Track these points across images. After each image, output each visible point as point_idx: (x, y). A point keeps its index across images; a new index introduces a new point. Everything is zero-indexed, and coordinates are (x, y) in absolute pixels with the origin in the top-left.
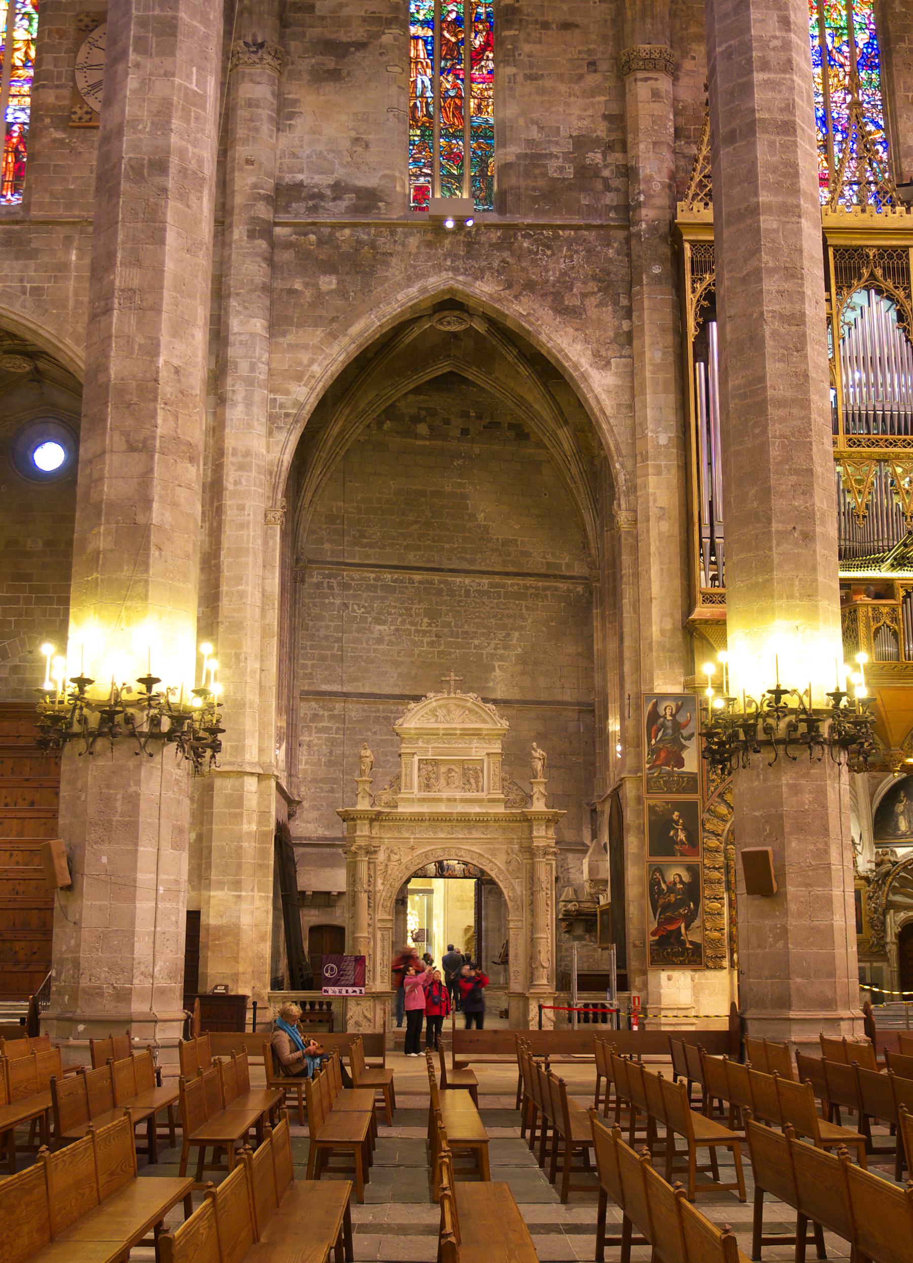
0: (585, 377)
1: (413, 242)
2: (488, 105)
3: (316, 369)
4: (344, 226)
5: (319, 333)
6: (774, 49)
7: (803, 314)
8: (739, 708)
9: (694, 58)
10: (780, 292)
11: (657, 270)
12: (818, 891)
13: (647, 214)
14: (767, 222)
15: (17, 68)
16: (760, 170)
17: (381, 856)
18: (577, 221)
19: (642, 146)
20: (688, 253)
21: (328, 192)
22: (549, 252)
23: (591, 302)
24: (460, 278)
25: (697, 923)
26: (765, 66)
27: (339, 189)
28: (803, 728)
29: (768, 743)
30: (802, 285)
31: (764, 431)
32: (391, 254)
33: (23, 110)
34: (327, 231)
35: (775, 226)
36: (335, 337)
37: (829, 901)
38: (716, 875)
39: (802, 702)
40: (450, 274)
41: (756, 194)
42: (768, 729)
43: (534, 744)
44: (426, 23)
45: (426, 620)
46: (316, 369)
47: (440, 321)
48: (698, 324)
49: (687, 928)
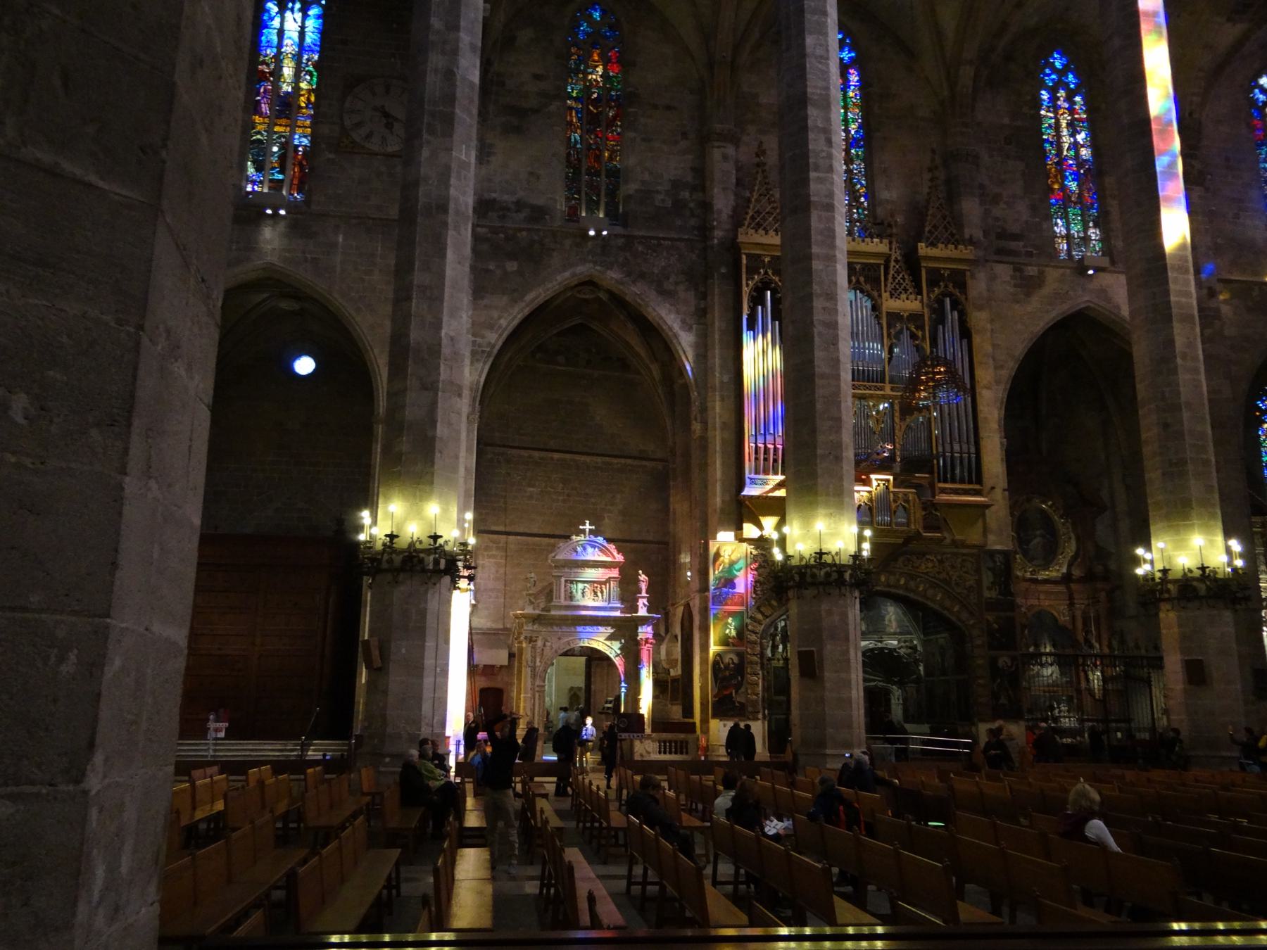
0: (676, 336)
1: (568, 243)
2: (616, 157)
3: (503, 322)
4: (521, 230)
5: (505, 299)
6: (823, 157)
7: (837, 323)
8: (794, 562)
9: (748, 134)
10: (824, 309)
11: (723, 270)
12: (843, 675)
13: (718, 234)
14: (817, 265)
15: (302, 108)
16: (813, 232)
17: (540, 643)
18: (673, 235)
19: (716, 190)
20: (744, 261)
22: (655, 254)
23: (681, 288)
24: (598, 268)
25: (743, 690)
26: (817, 169)
27: (519, 205)
28: (835, 576)
29: (813, 584)
30: (836, 305)
31: (813, 392)
32: (553, 250)
33: (305, 137)
34: (511, 232)
35: (821, 267)
36: (516, 302)
37: (850, 681)
38: (755, 658)
39: (834, 560)
40: (591, 265)
41: (810, 247)
42: (814, 576)
43: (640, 572)
44: (576, 99)
45: (561, 485)
46: (503, 322)
47: (579, 292)
48: (750, 306)
49: (736, 692)
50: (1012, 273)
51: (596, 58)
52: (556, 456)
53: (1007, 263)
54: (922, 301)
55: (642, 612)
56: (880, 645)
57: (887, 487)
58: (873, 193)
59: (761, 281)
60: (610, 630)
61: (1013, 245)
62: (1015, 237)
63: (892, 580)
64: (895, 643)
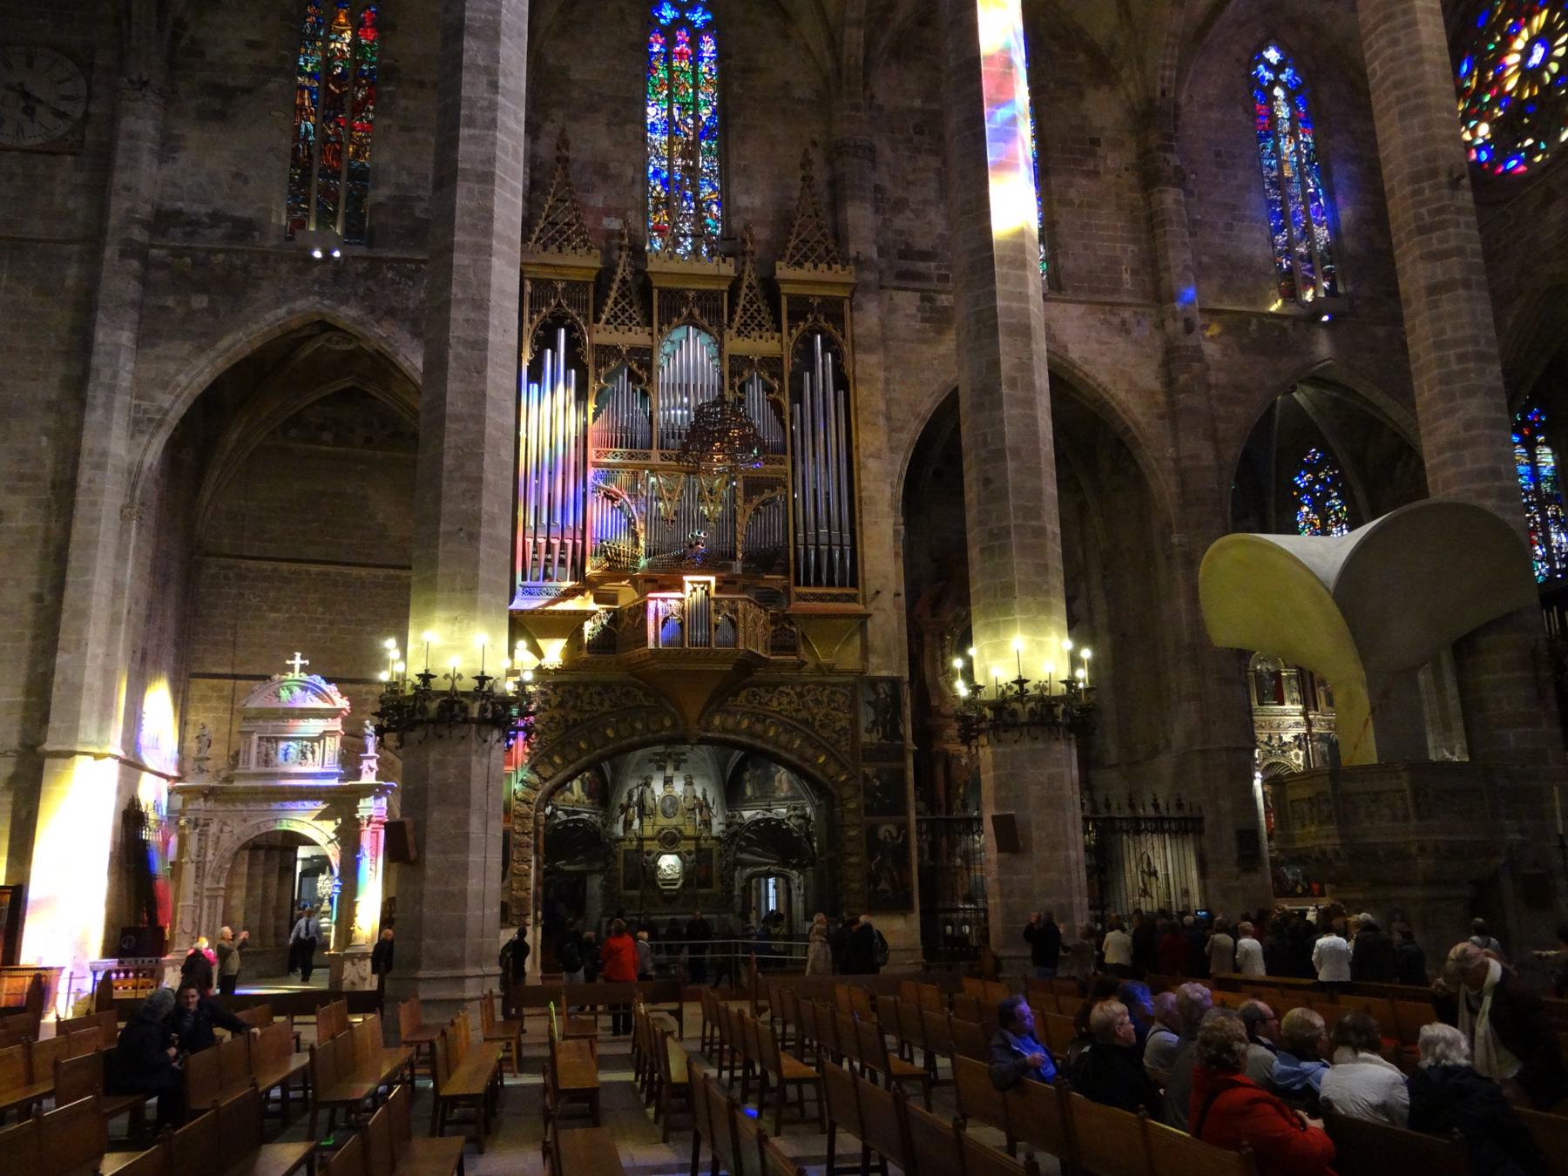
1: (284, 268)
2: (364, 153)
4: (220, 251)
5: (188, 347)
6: (481, 108)
7: (486, 341)
9: (553, 121)
10: (467, 321)
14: (459, 259)
16: (458, 212)
17: (213, 828)
21: (206, 220)
24: (326, 302)
26: (471, 123)
27: (216, 218)
30: (488, 315)
31: (442, 442)
32: (262, 278)
34: (202, 255)
35: (467, 262)
40: (317, 298)
44: (310, 75)
46: (182, 379)
47: (329, 340)
48: (533, 350)
50: (919, 303)
51: (343, 20)
52: (314, 568)
53: (914, 290)
54: (781, 341)
55: (368, 778)
56: (769, 815)
57: (707, 593)
58: (728, 199)
59: (552, 315)
60: (321, 806)
61: (921, 266)
62: (925, 256)
63: (730, 722)
64: (785, 810)
